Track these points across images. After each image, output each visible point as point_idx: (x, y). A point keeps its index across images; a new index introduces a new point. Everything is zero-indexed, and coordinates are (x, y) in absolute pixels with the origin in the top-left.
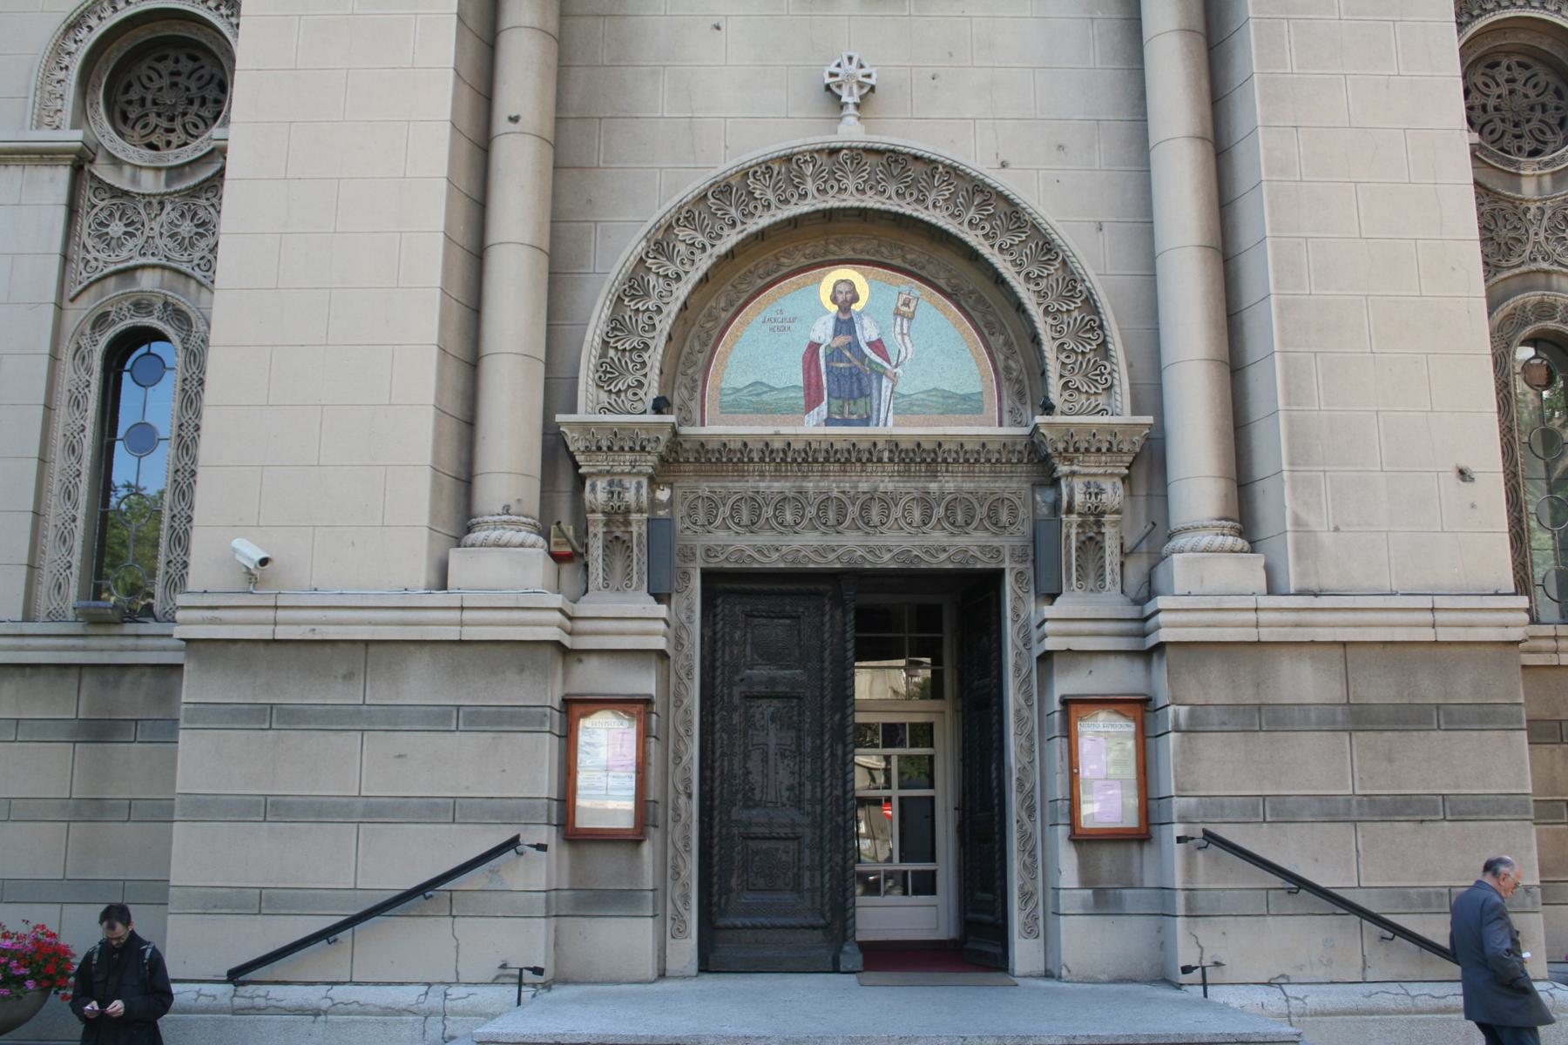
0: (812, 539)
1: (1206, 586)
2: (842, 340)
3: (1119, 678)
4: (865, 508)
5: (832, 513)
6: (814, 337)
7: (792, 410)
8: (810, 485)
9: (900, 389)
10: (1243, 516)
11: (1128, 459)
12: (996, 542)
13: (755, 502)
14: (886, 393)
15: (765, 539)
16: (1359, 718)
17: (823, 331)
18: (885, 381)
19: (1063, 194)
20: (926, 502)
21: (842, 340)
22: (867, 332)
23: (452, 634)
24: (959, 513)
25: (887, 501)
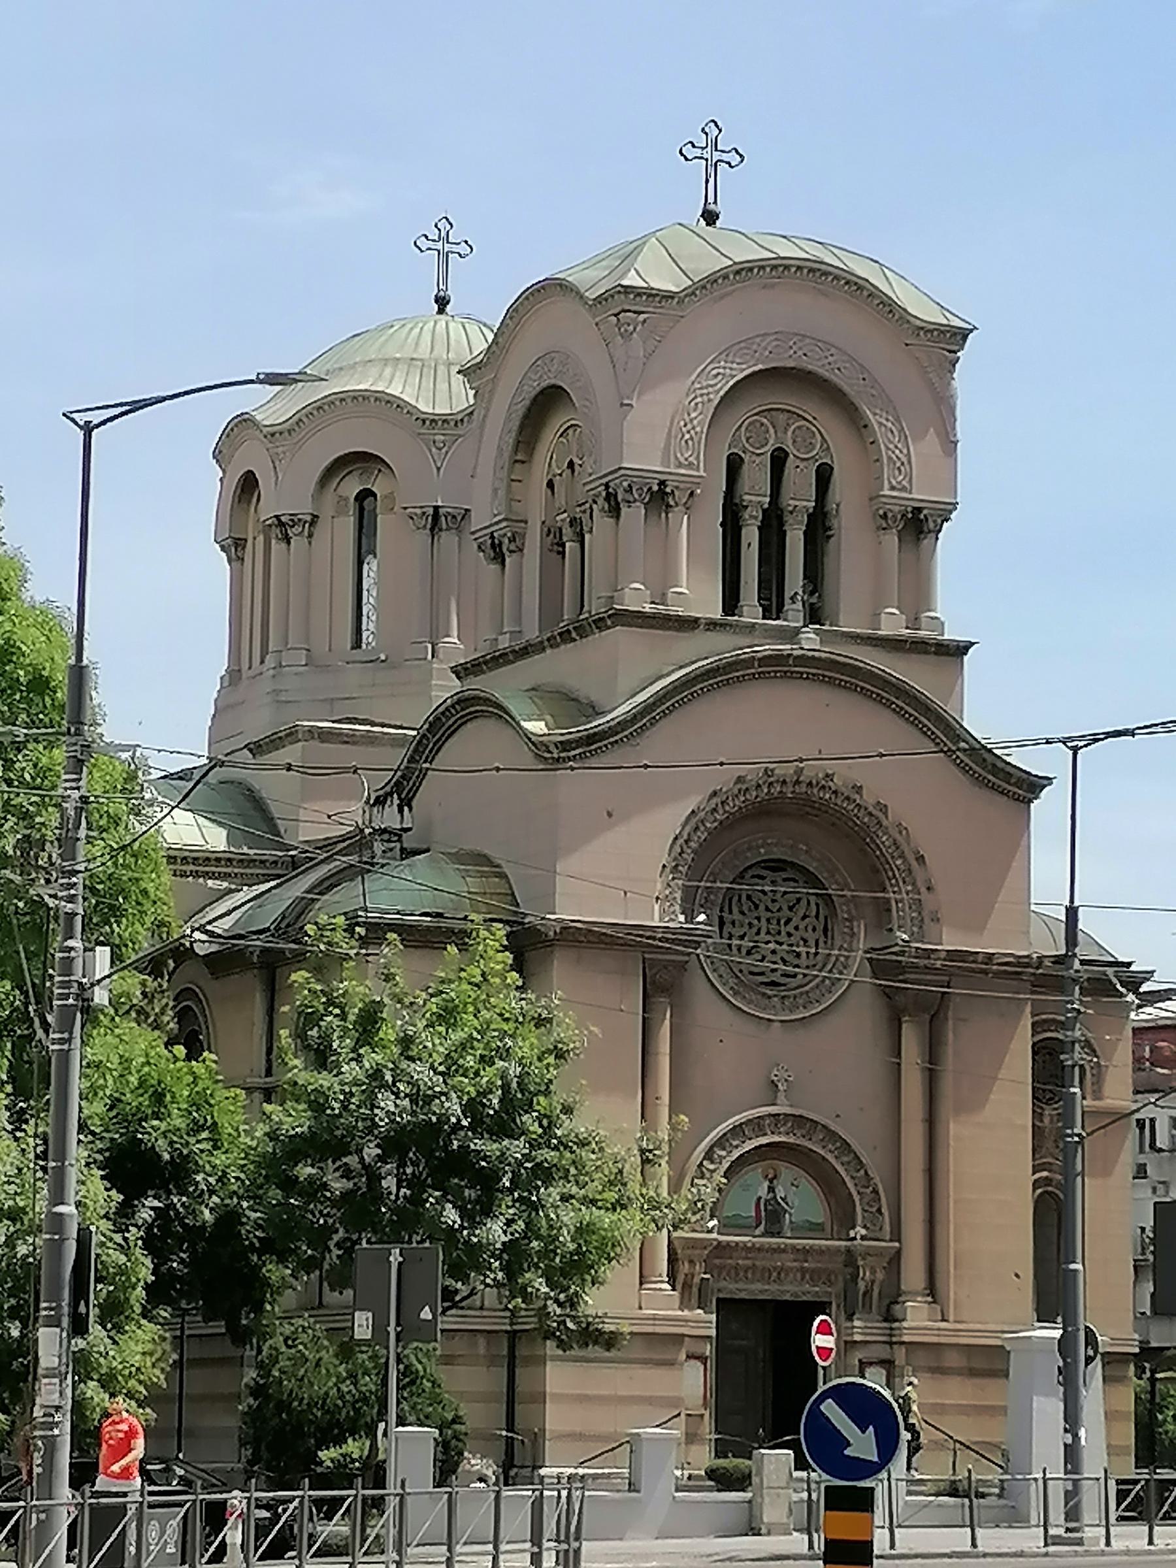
0: (759, 1286)
1: (916, 1318)
2: (771, 1195)
3: (883, 1352)
4: (779, 1274)
5: (766, 1274)
6: (760, 1194)
7: (749, 1227)
8: (758, 1263)
9: (793, 1220)
10: (932, 1290)
11: (887, 1259)
12: (829, 1290)
13: (736, 1268)
14: (787, 1221)
15: (740, 1285)
16: (973, 1373)
17: (763, 1191)
18: (787, 1216)
19: (861, 1131)
20: (803, 1271)
21: (771, 1195)
22: (780, 1193)
23: (650, 1329)
24: (815, 1276)
25: (788, 1271)
